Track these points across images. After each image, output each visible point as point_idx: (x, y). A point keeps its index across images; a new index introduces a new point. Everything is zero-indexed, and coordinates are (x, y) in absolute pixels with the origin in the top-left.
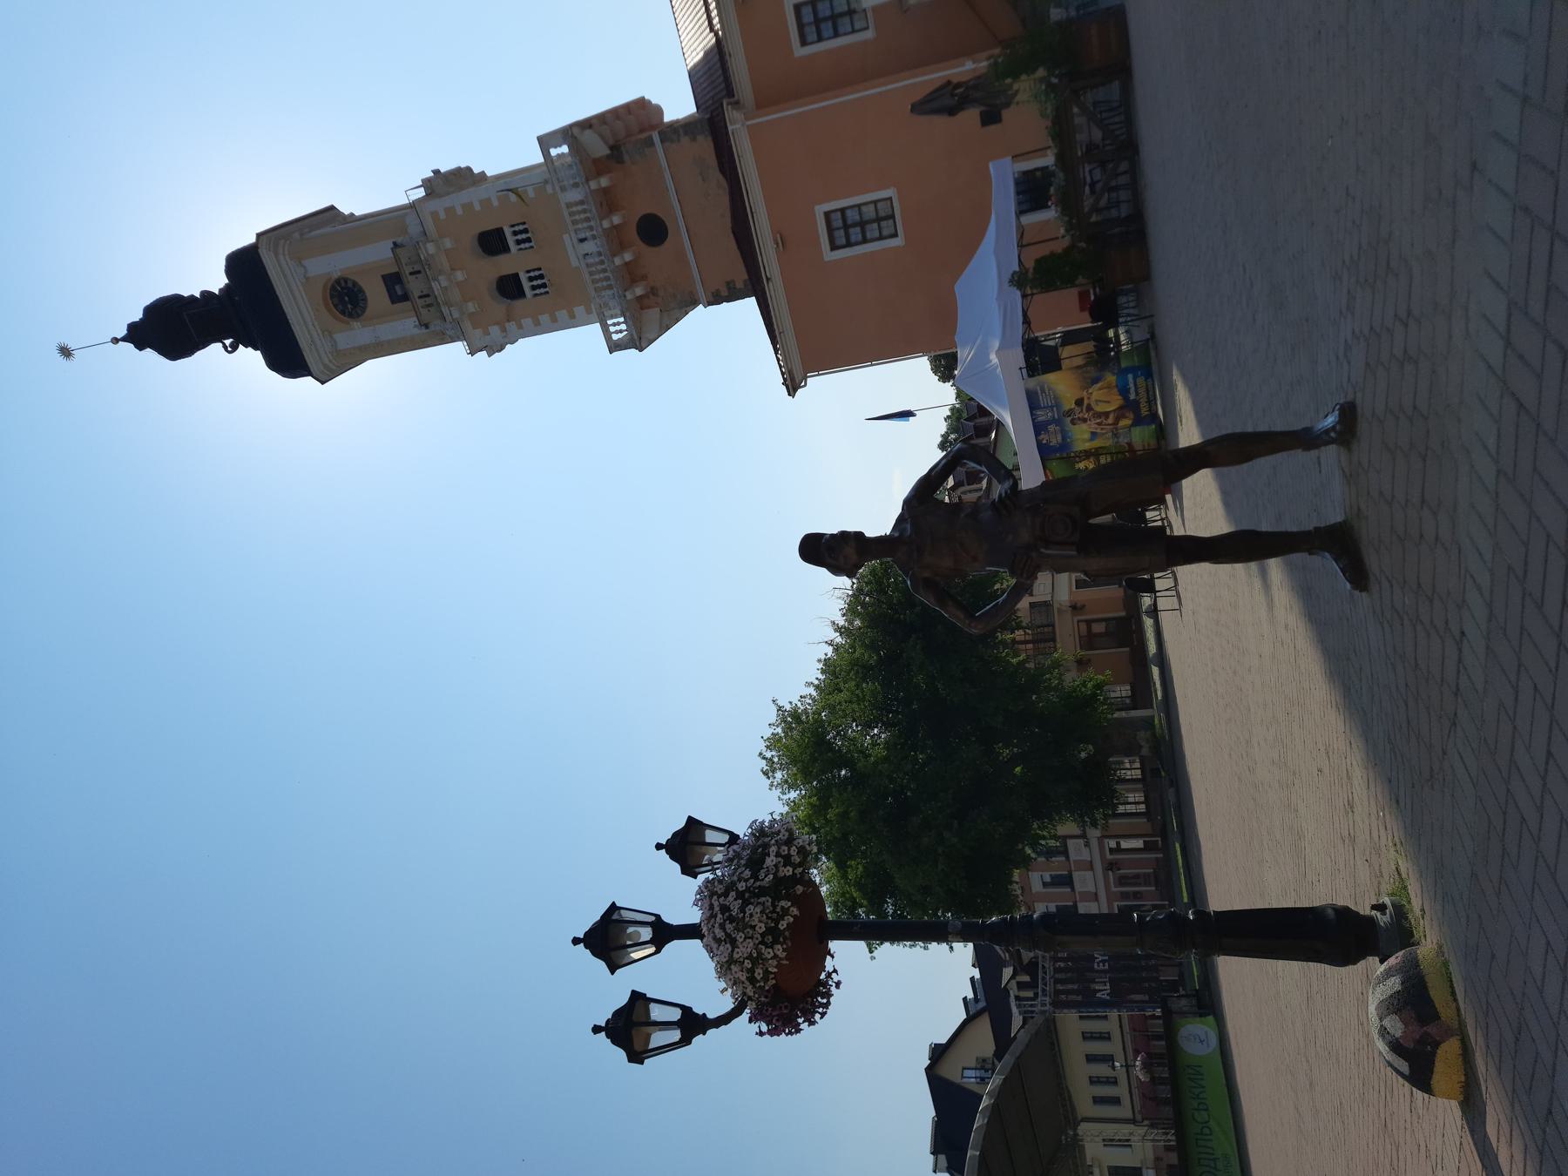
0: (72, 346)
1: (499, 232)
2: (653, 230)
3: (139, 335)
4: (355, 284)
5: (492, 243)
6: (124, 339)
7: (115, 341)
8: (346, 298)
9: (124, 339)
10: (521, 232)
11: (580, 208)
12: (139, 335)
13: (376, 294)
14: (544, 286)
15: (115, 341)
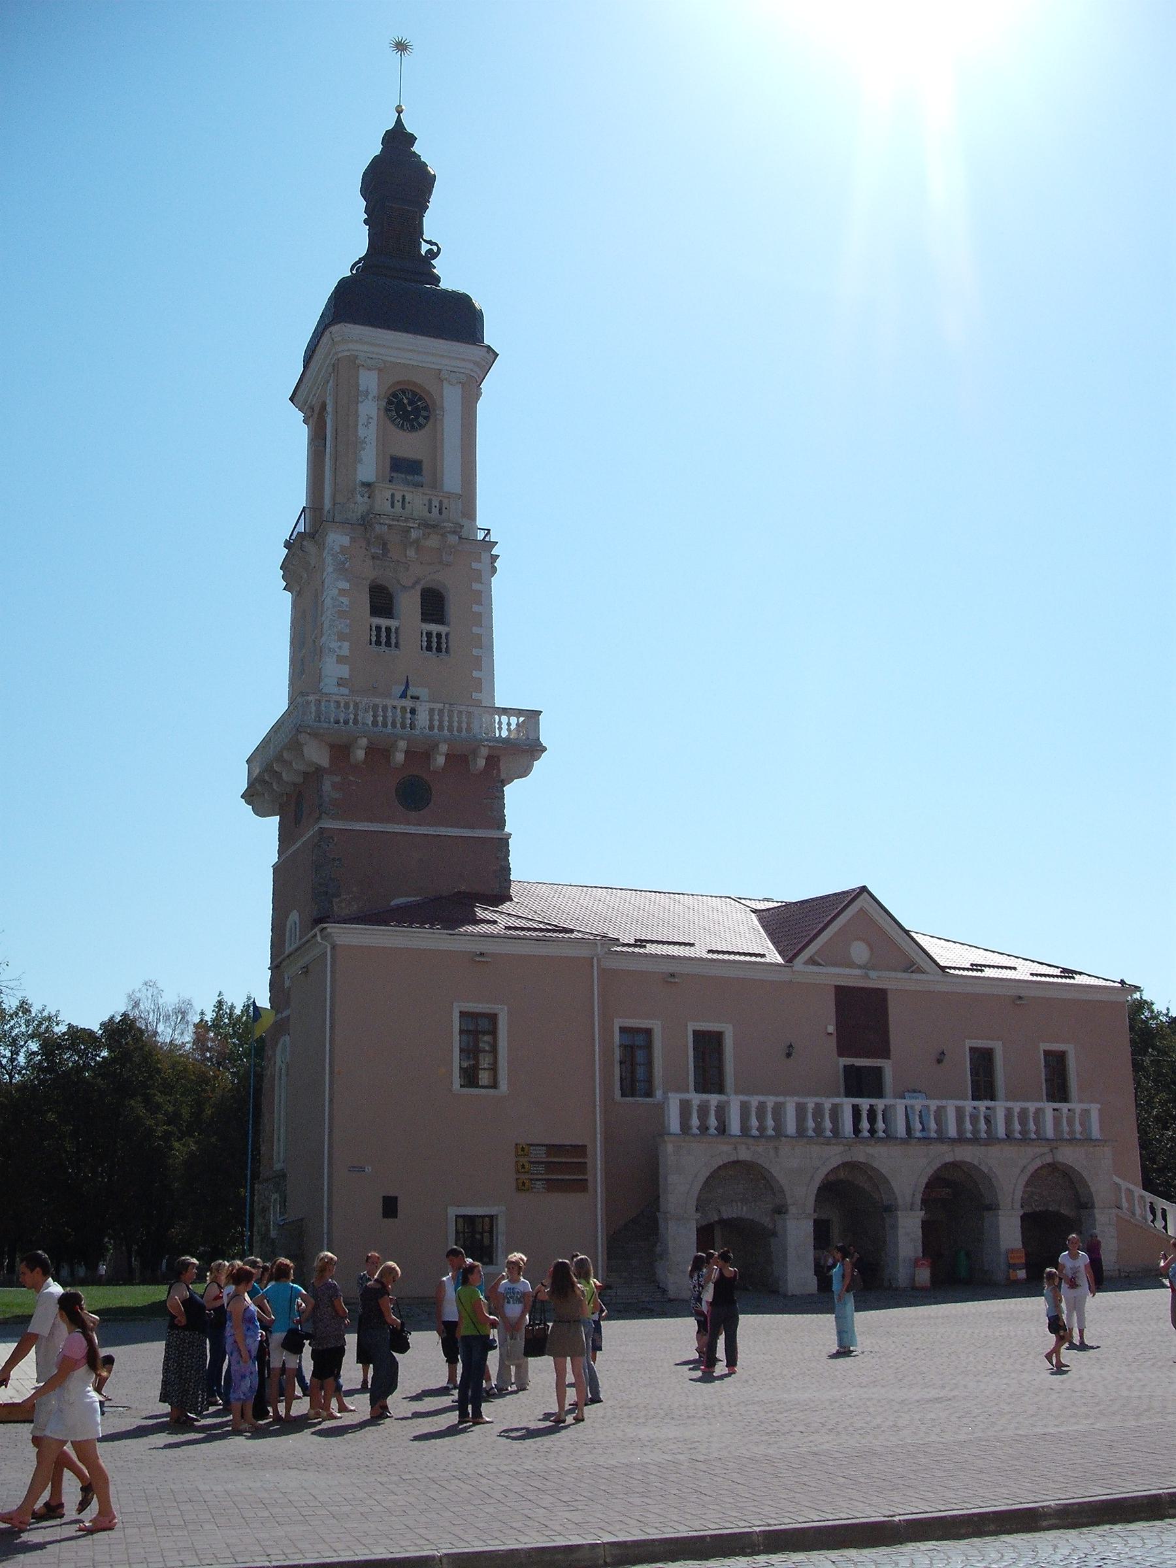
0: (406, 57)
1: (440, 619)
2: (414, 794)
3: (398, 141)
4: (421, 426)
5: (434, 605)
6: (399, 121)
7: (400, 111)
8: (409, 407)
9: (399, 121)
10: (439, 643)
11: (464, 726)
12: (398, 141)
13: (409, 444)
14: (378, 643)
15: (400, 111)
